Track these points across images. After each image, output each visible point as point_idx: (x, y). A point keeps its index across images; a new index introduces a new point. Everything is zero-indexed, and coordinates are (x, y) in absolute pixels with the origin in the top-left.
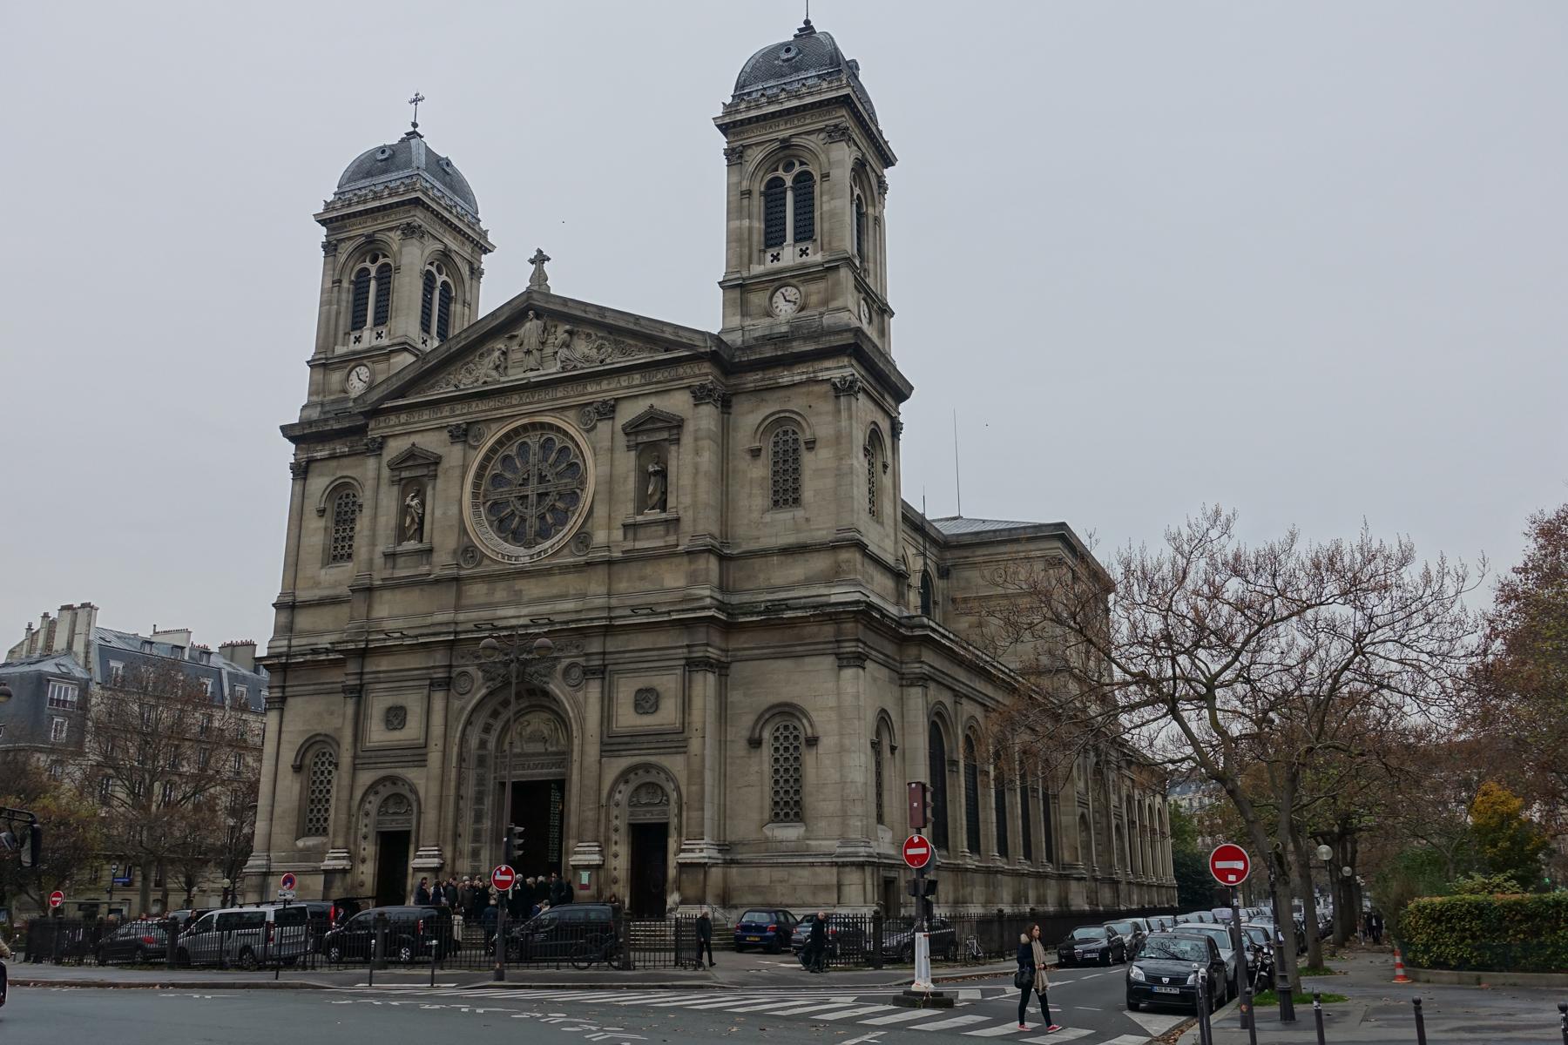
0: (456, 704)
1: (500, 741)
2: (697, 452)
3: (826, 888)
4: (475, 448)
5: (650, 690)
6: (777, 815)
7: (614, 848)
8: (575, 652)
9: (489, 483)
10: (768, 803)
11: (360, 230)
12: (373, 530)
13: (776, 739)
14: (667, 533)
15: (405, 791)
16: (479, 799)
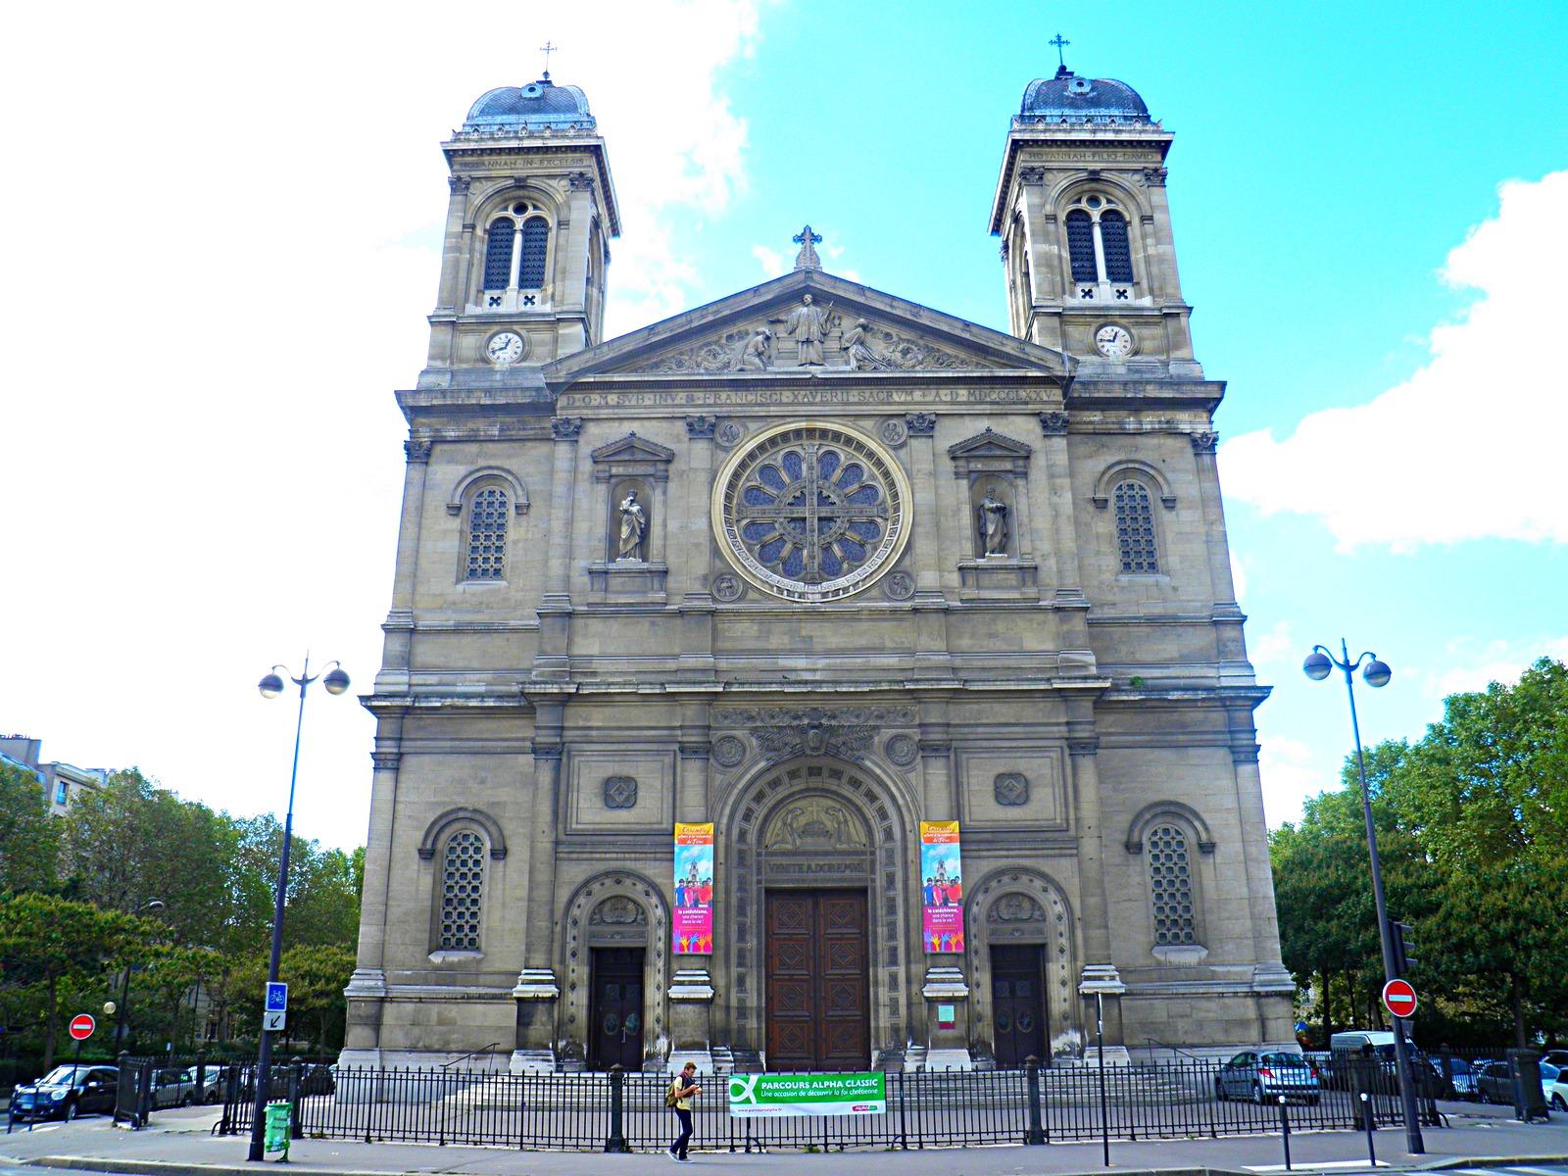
0: (719, 778)
1: (761, 832)
2: (1054, 491)
3: (1243, 1023)
4: (726, 450)
5: (1015, 776)
6: (1163, 936)
7: (976, 975)
8: (901, 721)
9: (745, 498)
10: (1153, 922)
11: (507, 170)
12: (569, 535)
13: (1155, 844)
16: (742, 910)
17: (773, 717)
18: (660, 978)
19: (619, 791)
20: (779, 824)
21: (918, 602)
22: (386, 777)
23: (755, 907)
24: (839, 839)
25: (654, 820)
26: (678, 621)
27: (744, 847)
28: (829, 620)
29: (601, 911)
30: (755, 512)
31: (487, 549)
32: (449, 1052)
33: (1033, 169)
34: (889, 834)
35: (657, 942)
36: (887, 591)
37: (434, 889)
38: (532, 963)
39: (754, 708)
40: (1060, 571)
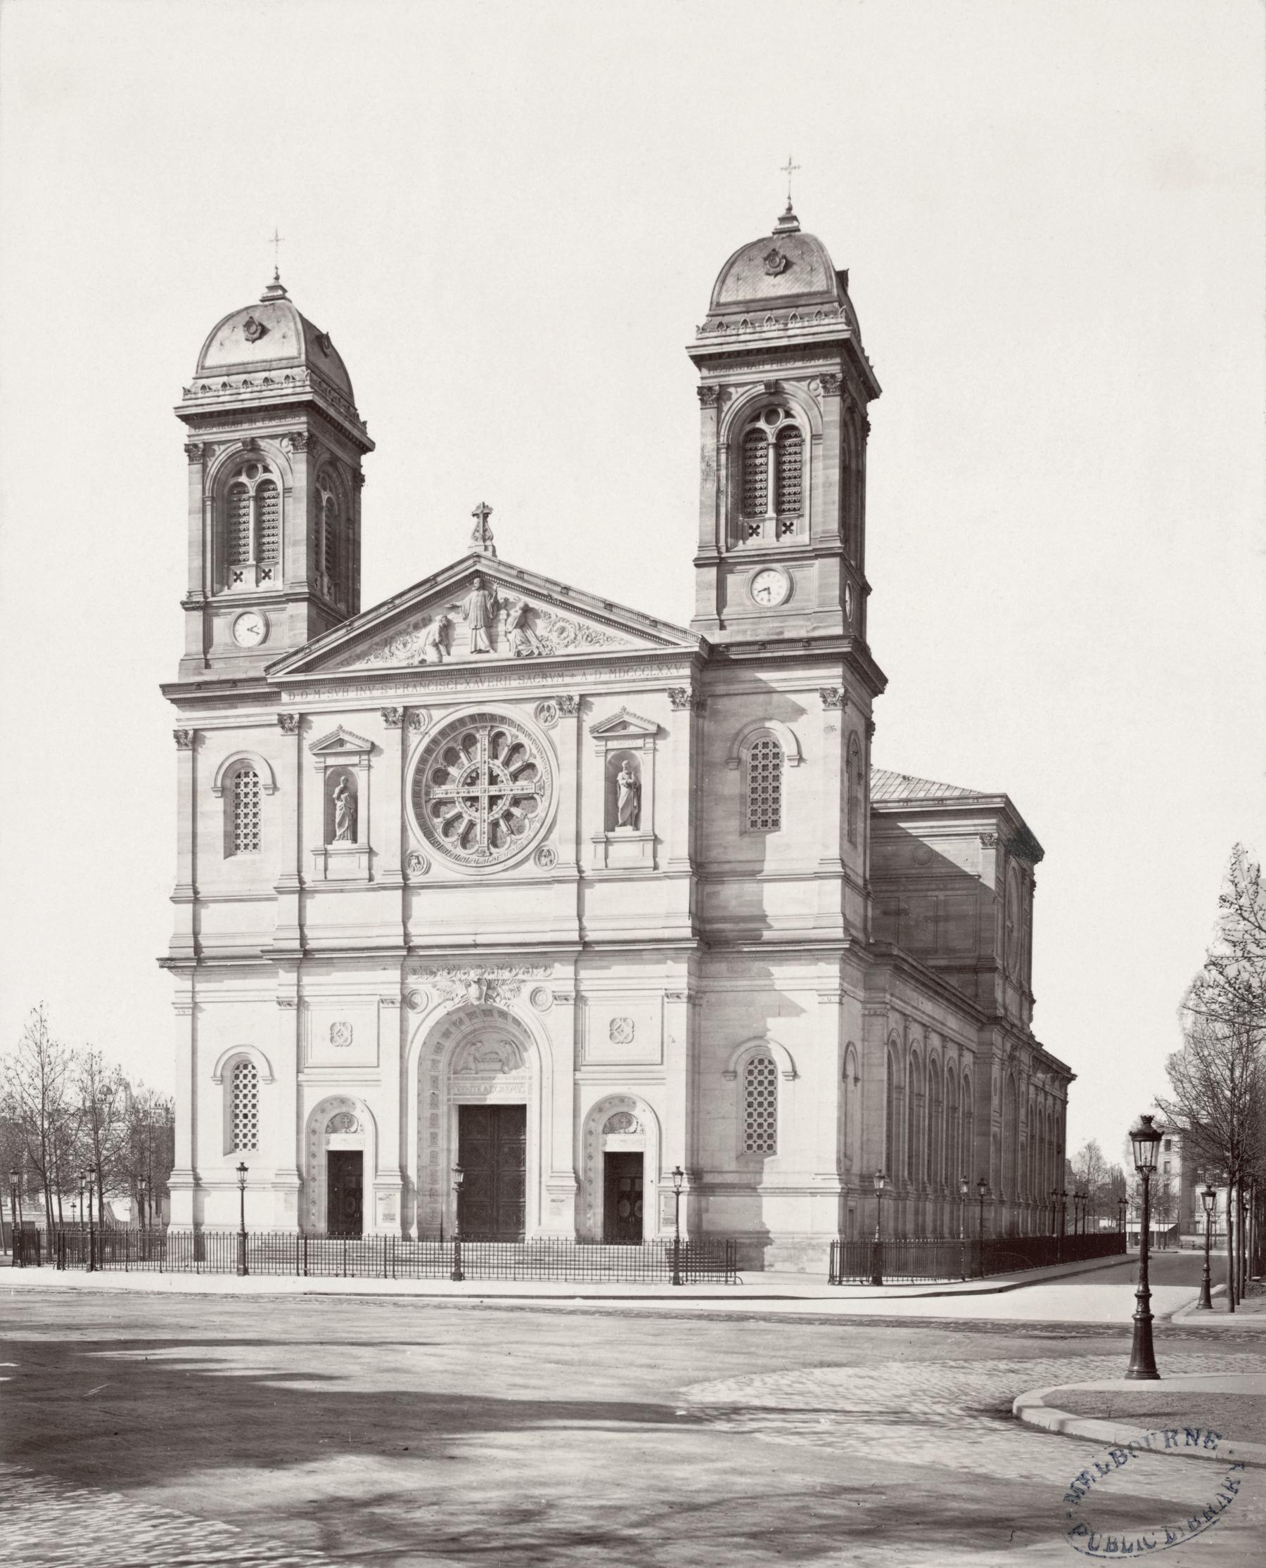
33: (710, 389)
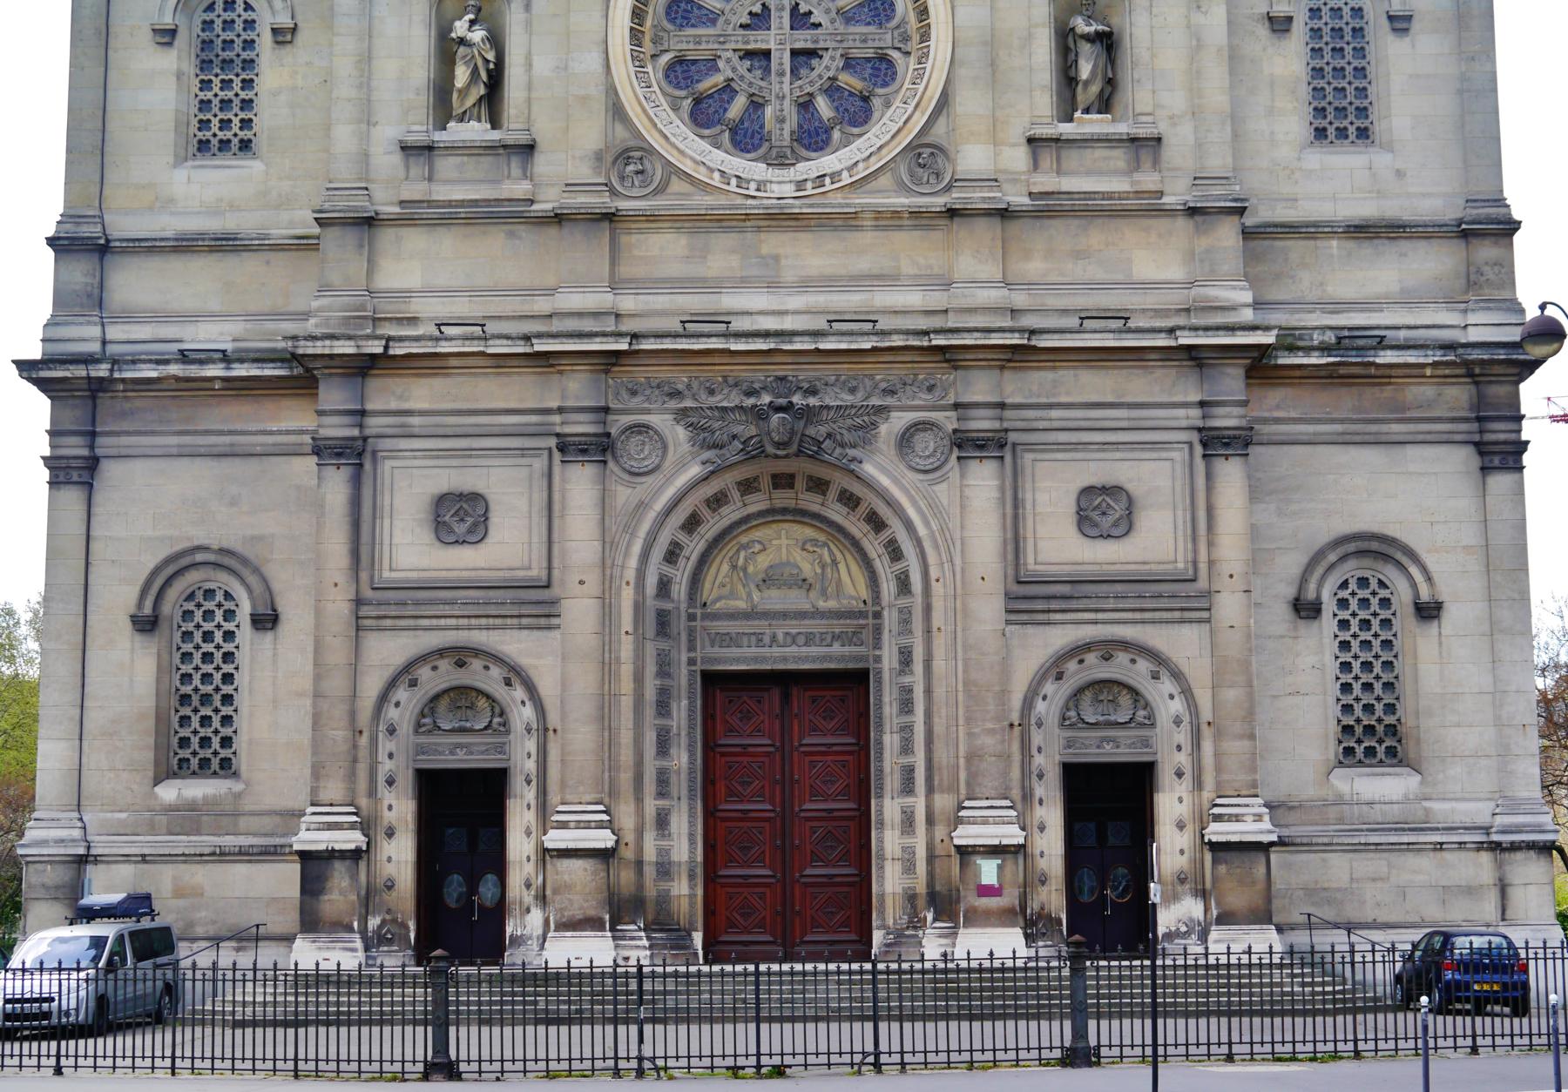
0: (624, 495)
3: (1470, 891)
5: (1112, 490)
6: (1349, 751)
8: (924, 398)
10: (1333, 729)
12: (365, 82)
13: (1343, 603)
14: (1136, 166)
15: (491, 680)
16: (663, 707)
17: (711, 392)
18: (530, 817)
19: (459, 515)
20: (725, 567)
21: (955, 198)
22: (73, 497)
23: (684, 703)
24: (824, 593)
25: (518, 564)
26: (553, 231)
27: (668, 606)
28: (806, 228)
29: (433, 711)
30: (685, 41)
31: (225, 104)
32: (194, 940)
34: (904, 585)
35: (522, 757)
36: (906, 178)
37: (158, 681)
38: (324, 796)
39: (681, 378)
40: (1199, 145)
